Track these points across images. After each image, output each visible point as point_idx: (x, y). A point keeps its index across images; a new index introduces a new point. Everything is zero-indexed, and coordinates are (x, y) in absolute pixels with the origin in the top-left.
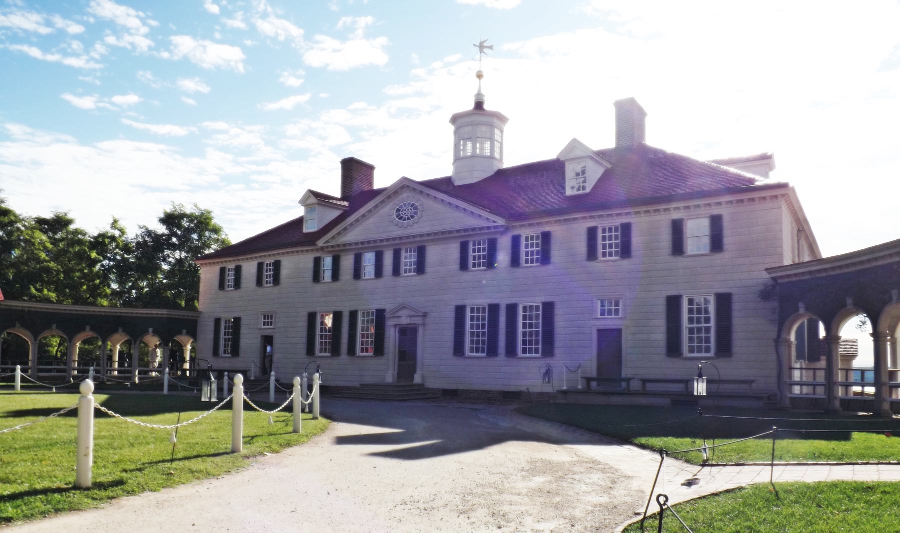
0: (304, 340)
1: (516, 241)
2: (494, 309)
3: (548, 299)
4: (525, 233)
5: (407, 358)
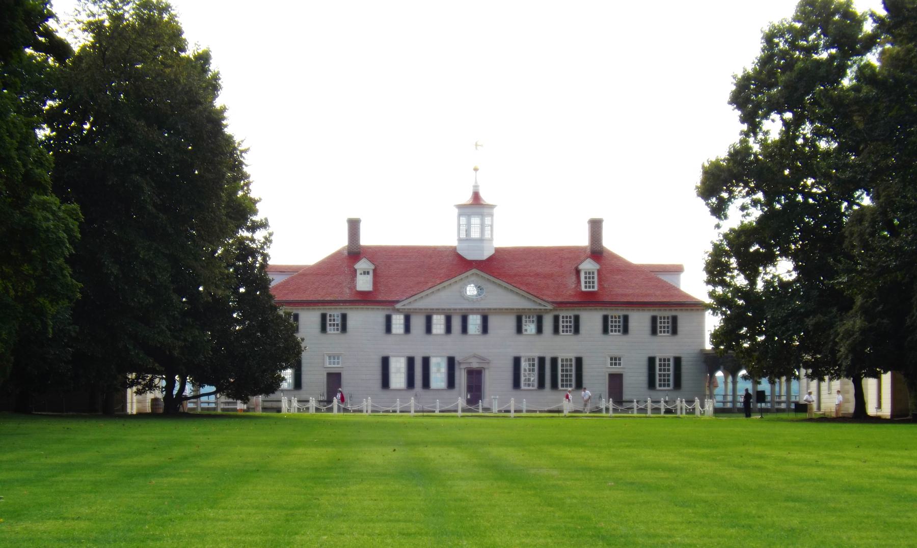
1: (556, 319)
2: (542, 360)
3: (579, 355)
4: (562, 314)
5: (475, 390)
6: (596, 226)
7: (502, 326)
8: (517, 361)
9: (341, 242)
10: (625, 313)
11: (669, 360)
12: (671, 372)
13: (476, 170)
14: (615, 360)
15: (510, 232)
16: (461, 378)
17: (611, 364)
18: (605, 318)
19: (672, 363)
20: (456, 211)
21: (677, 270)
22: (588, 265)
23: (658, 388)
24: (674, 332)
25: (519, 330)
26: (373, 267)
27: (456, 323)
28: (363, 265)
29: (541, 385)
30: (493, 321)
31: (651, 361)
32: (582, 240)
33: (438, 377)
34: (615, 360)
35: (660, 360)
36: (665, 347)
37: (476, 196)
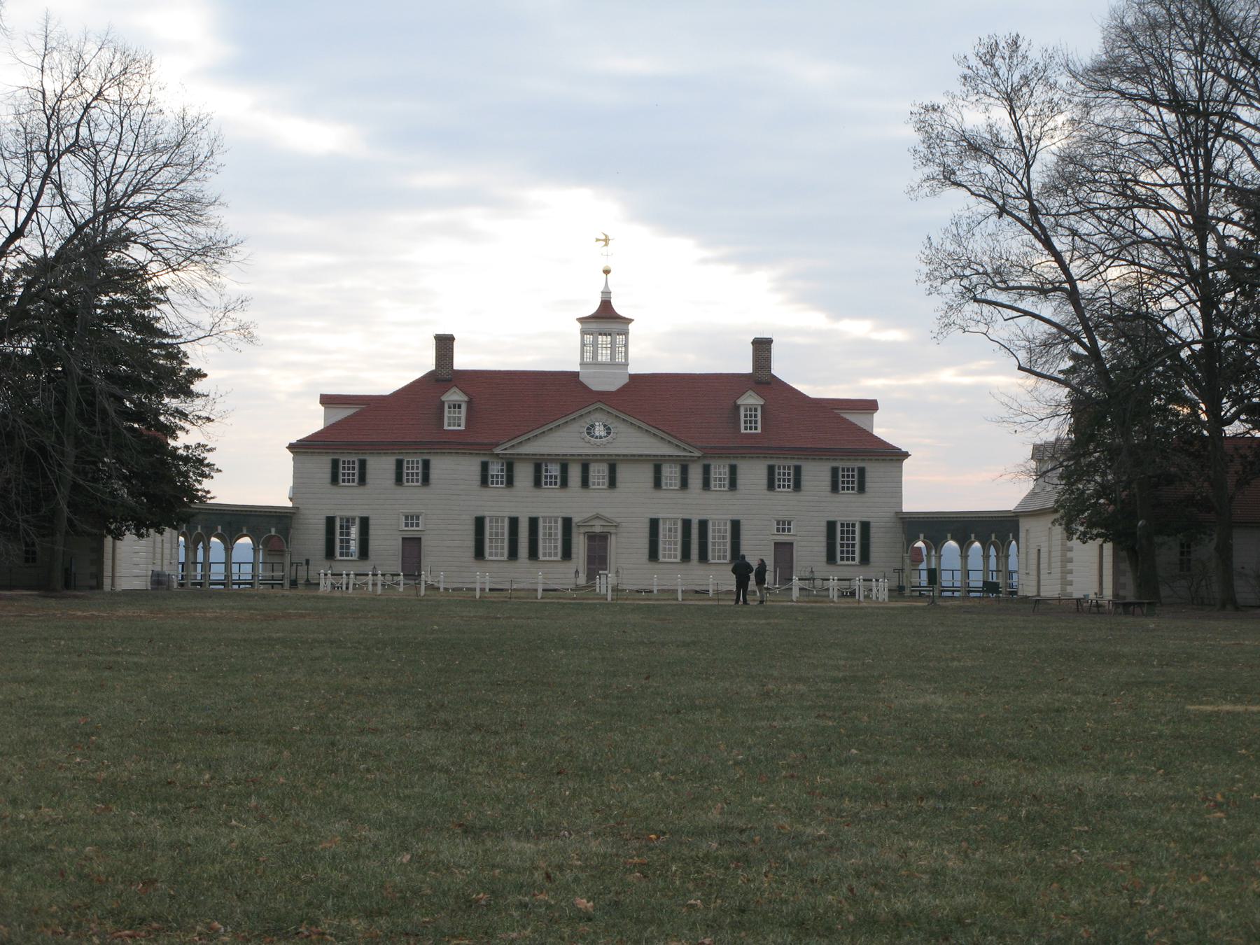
0: (470, 542)
1: (706, 470)
5: (598, 560)
6: (762, 347)
7: (635, 480)
8: (654, 524)
9: (427, 362)
10: (797, 463)
11: (854, 526)
12: (857, 541)
13: (607, 272)
14: (784, 525)
15: (648, 352)
16: (580, 545)
17: (778, 530)
18: (771, 470)
19: (857, 529)
20: (578, 326)
21: (870, 406)
22: (750, 400)
23: (839, 562)
24: (862, 489)
25: (657, 484)
26: (466, 399)
27: (575, 473)
28: (454, 396)
29: (686, 556)
30: (623, 473)
31: (831, 526)
32: (745, 366)
33: (550, 544)
34: (784, 525)
35: (842, 525)
36: (849, 508)
37: (606, 305)
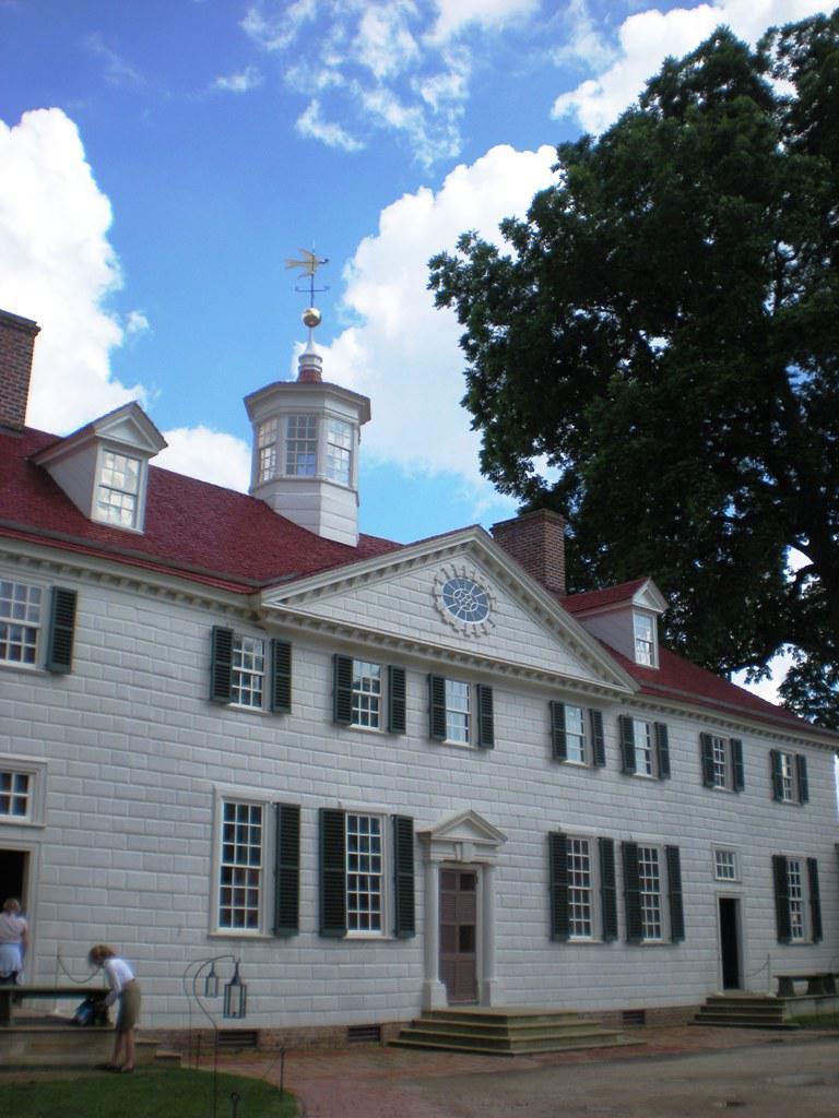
29: (609, 931)
